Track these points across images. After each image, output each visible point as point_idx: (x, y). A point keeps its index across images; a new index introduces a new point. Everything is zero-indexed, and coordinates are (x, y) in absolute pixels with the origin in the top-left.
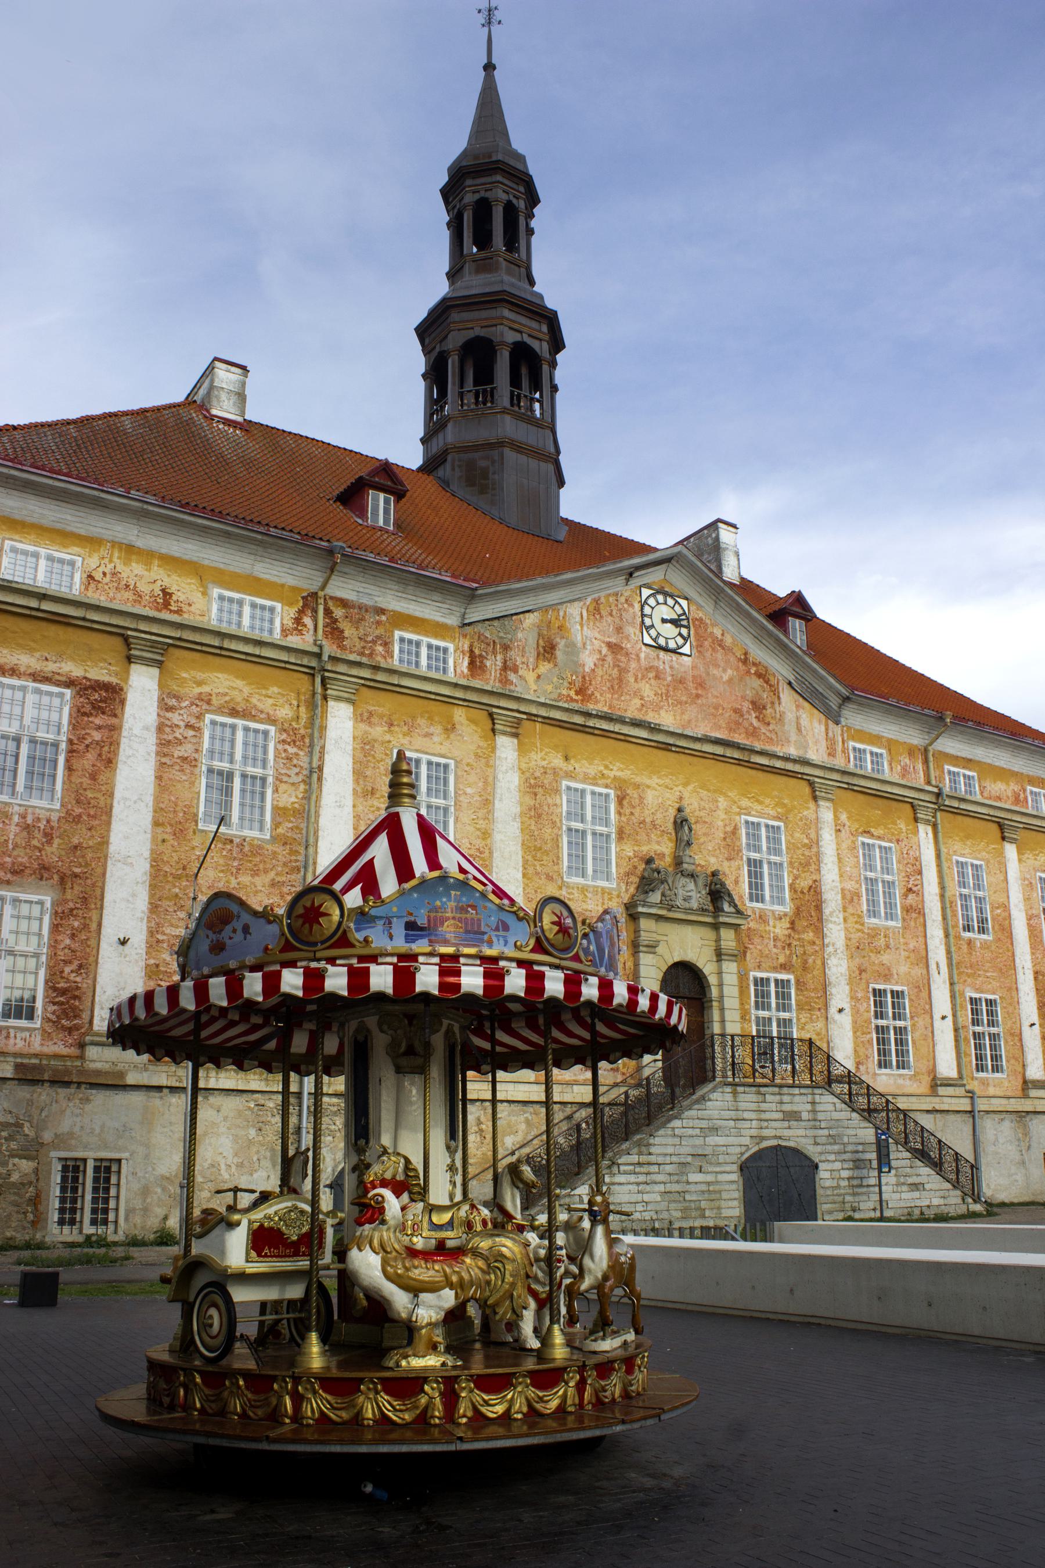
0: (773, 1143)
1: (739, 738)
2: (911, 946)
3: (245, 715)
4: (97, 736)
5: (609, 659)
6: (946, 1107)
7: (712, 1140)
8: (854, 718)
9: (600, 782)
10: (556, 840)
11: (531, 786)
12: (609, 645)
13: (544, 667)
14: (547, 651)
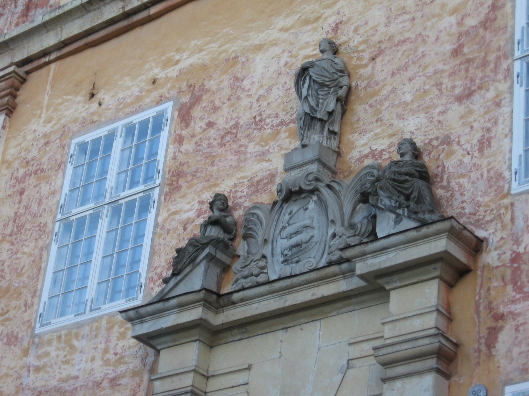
9: (148, 100)
11: (18, 180)
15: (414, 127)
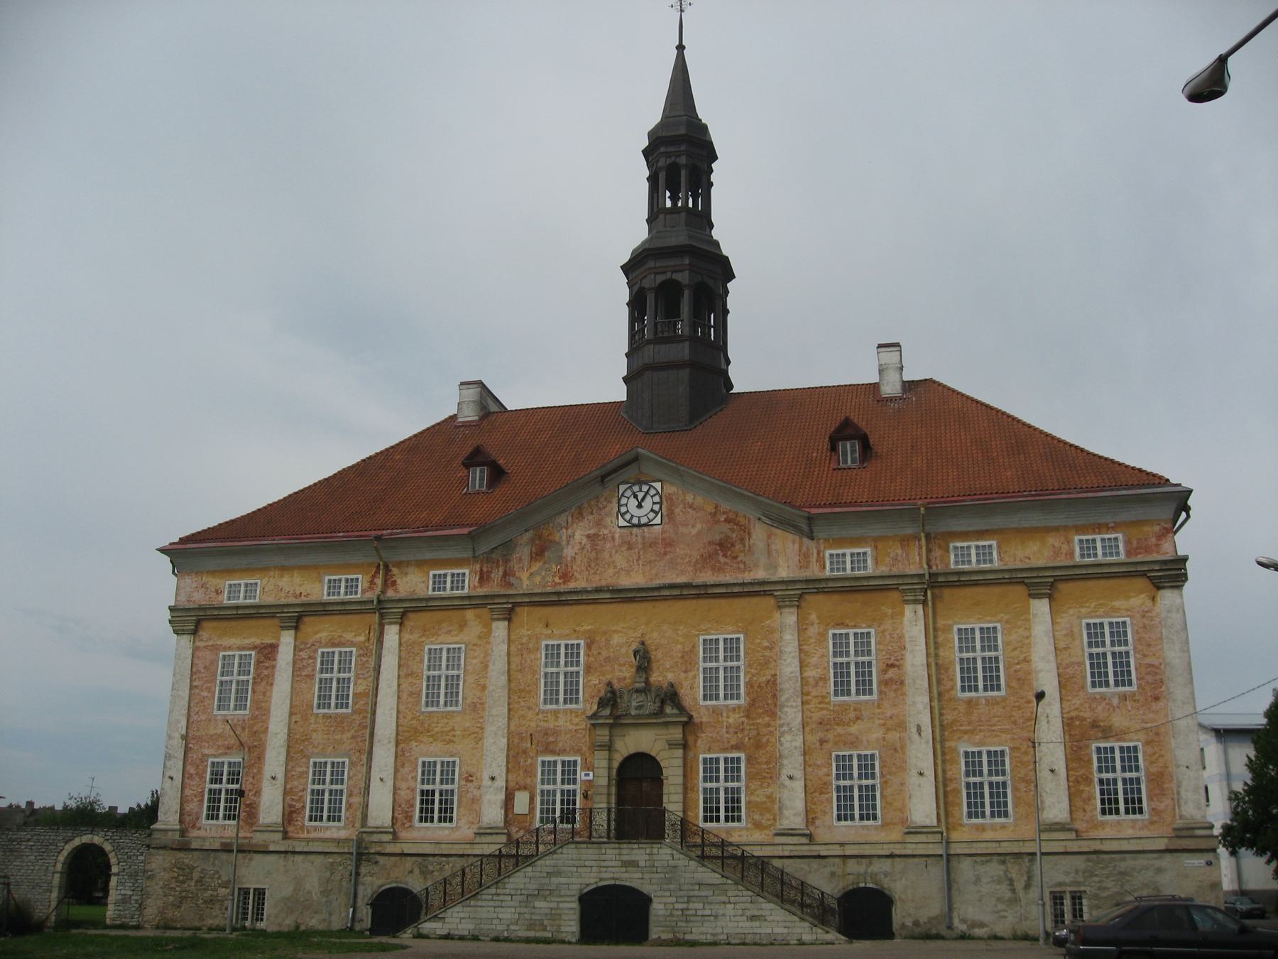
0: (612, 882)
1: (707, 577)
2: (889, 714)
3: (338, 645)
4: (266, 672)
5: (588, 547)
6: (909, 852)
7: (555, 880)
10: (536, 684)
12: (588, 536)
13: (537, 566)
15: (670, 677)
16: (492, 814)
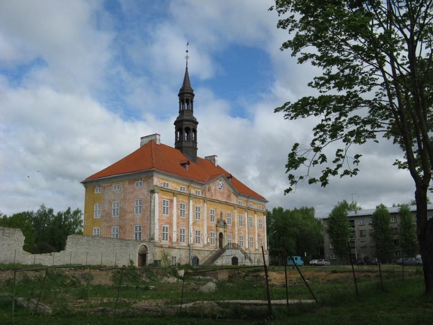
8: (239, 197)
14: (209, 190)
16: (206, 242)
